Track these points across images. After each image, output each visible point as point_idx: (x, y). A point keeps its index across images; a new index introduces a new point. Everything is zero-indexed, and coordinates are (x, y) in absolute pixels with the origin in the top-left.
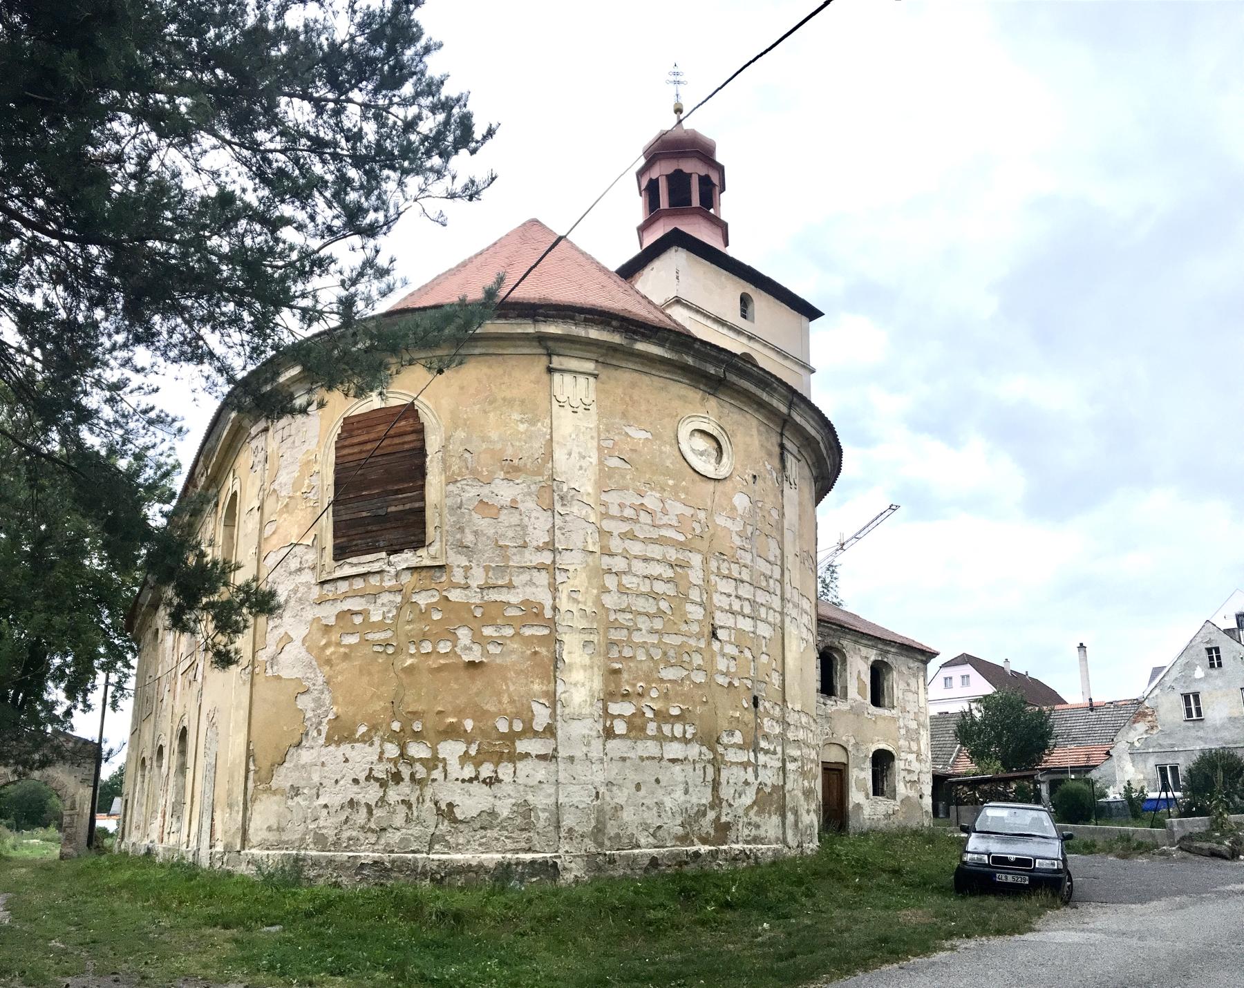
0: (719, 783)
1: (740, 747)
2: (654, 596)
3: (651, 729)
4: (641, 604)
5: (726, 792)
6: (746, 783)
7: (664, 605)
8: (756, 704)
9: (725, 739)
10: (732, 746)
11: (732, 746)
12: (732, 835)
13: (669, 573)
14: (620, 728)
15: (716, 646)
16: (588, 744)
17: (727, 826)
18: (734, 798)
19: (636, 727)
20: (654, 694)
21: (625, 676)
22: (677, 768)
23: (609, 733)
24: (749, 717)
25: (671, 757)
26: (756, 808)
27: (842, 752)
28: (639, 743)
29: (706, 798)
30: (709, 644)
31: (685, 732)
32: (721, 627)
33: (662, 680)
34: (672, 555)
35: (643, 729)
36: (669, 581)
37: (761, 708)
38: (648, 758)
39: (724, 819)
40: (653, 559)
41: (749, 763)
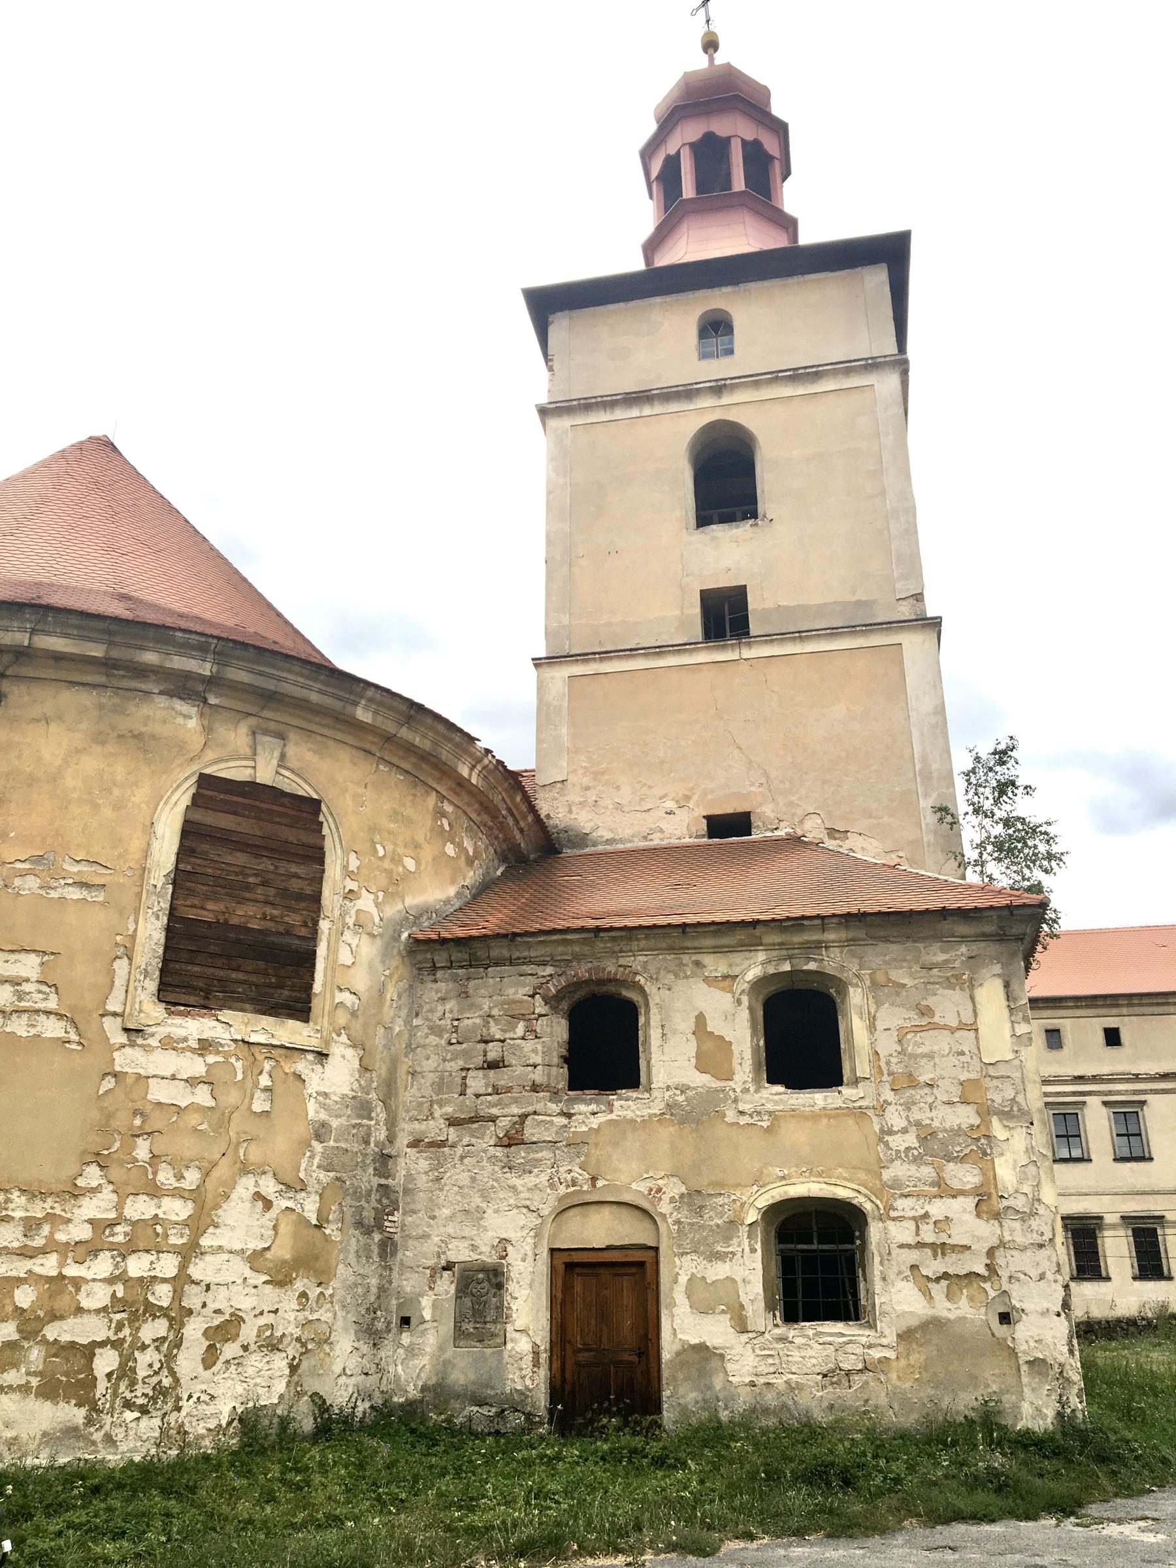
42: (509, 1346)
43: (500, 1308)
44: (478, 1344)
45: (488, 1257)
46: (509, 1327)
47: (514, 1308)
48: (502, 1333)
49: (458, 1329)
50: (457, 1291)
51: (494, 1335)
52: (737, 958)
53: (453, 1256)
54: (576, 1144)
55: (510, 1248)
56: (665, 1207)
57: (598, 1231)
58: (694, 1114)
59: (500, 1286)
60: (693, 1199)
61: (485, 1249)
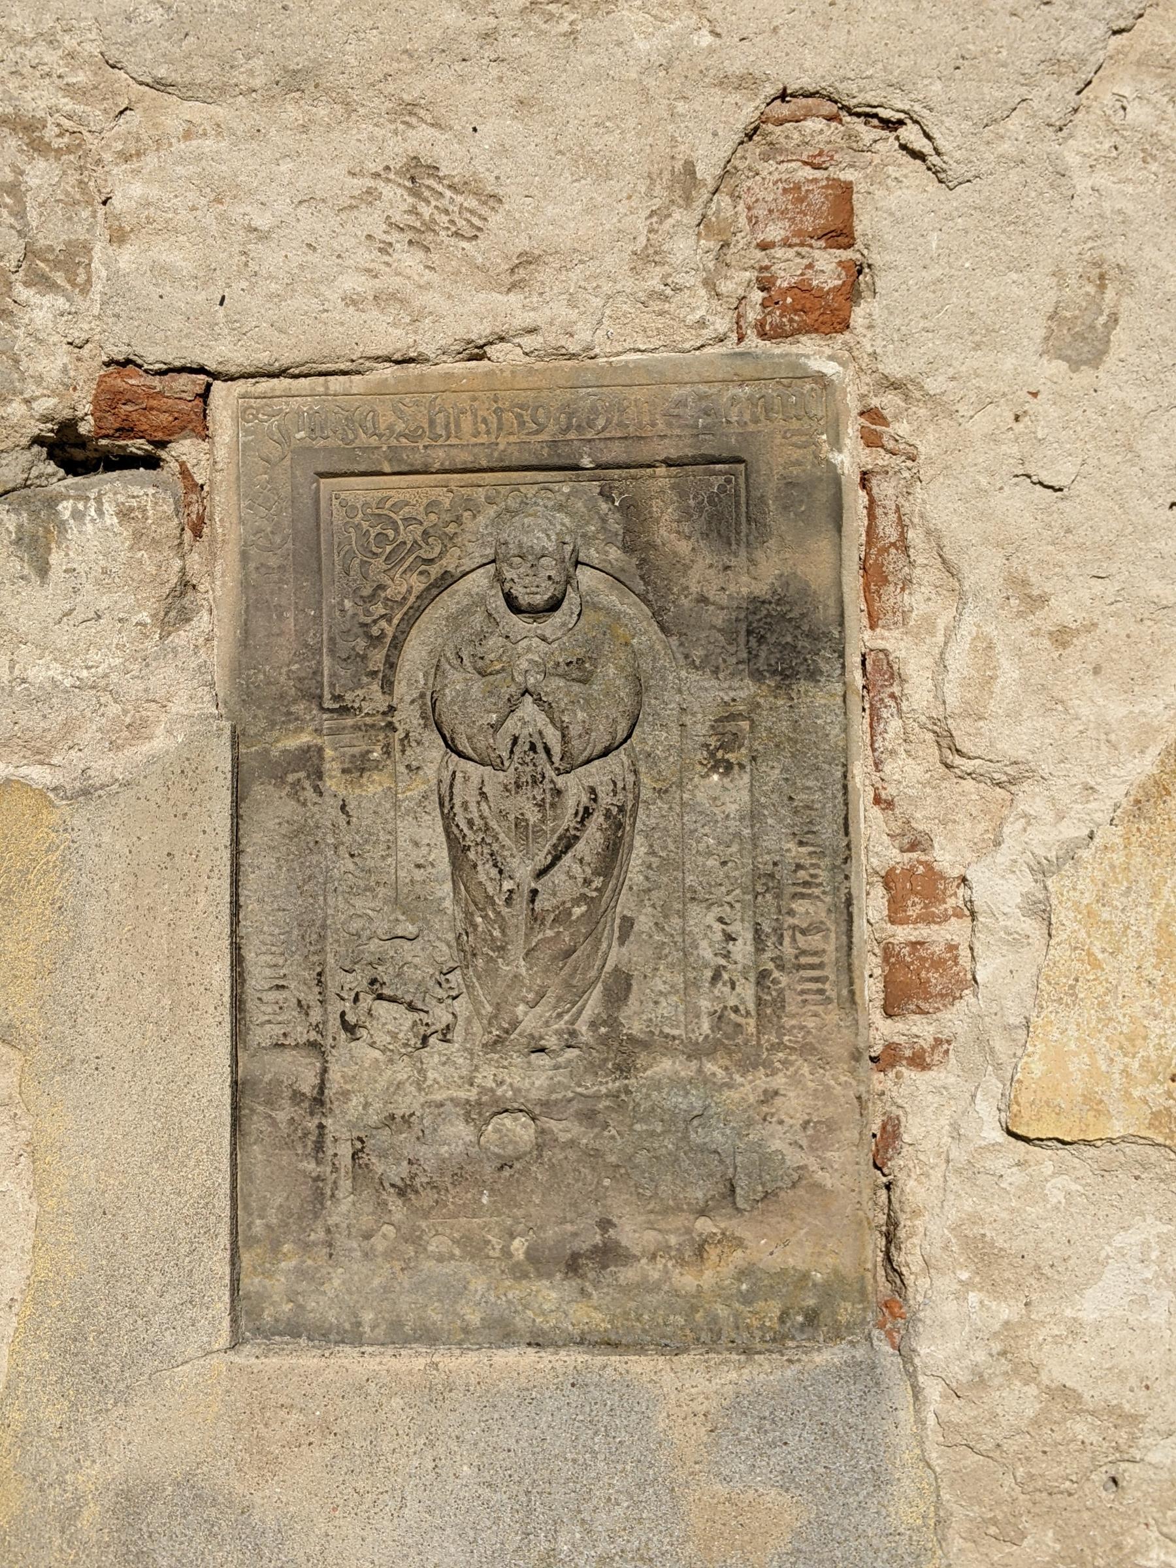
42: (952, 1322)
43: (801, 875)
44: (550, 1298)
45: (620, 299)
46: (937, 1112)
47: (999, 887)
48: (841, 1166)
49: (277, 1115)
50: (253, 700)
51: (744, 1187)
53: (162, 289)
55: (893, 202)
59: (784, 642)
61: (560, 209)
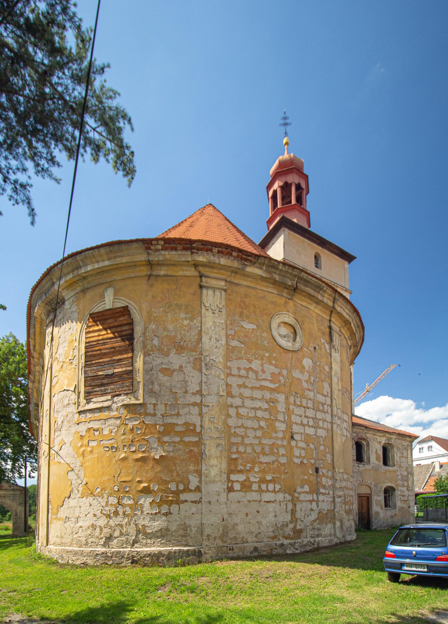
0: (296, 511)
1: (307, 493)
2: (258, 419)
3: (255, 487)
4: (249, 423)
5: (298, 515)
6: (312, 510)
7: (263, 424)
8: (317, 470)
9: (299, 490)
10: (303, 493)
11: (303, 493)
12: (304, 534)
13: (266, 406)
14: (237, 486)
15: (293, 443)
16: (219, 495)
17: (301, 531)
18: (304, 518)
19: (246, 486)
20: (257, 469)
21: (240, 461)
22: (270, 505)
23: (230, 490)
24: (313, 478)
25: (266, 500)
26: (318, 521)
27: (369, 490)
28: (247, 493)
29: (288, 518)
30: (289, 443)
31: (275, 488)
32: (296, 433)
33: (261, 463)
34: (268, 395)
35: (250, 487)
36: (266, 410)
37: (320, 473)
38: (252, 501)
39: (298, 527)
40: (256, 398)
41: (313, 500)
52: (381, 438)
54: (361, 473)
56: (372, 486)
57: (364, 490)
58: (376, 469)
60: (376, 485)
